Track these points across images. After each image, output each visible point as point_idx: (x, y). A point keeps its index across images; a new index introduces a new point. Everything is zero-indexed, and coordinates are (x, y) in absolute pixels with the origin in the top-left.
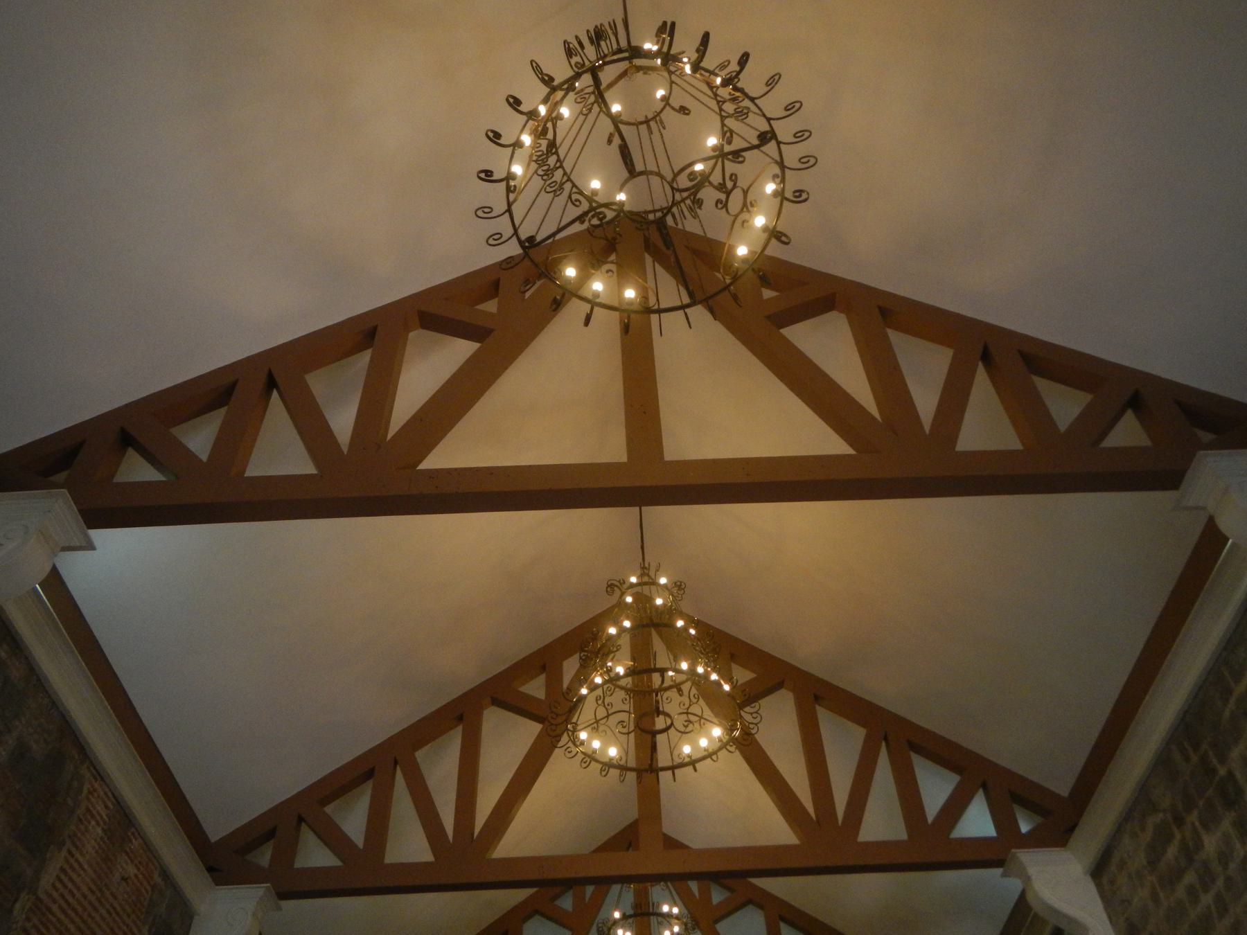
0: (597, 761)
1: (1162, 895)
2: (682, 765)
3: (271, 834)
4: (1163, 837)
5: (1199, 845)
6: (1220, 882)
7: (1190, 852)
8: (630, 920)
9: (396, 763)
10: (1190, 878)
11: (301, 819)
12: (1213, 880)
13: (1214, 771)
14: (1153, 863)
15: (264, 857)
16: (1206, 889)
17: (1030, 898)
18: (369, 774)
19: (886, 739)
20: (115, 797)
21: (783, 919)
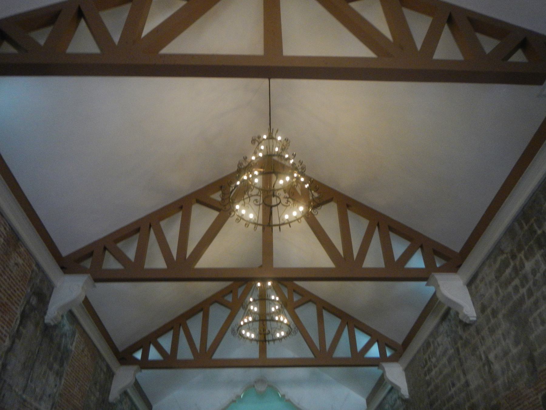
0: (243, 219)
1: (500, 291)
2: (284, 224)
3: (91, 254)
4: (505, 264)
8: (257, 302)
9: (150, 226)
10: (516, 282)
11: (105, 249)
12: (527, 282)
13: (535, 232)
14: (497, 278)
15: (87, 264)
16: (523, 286)
17: (438, 295)
18: (138, 230)
19: (378, 225)
20: (10, 225)
21: (324, 308)
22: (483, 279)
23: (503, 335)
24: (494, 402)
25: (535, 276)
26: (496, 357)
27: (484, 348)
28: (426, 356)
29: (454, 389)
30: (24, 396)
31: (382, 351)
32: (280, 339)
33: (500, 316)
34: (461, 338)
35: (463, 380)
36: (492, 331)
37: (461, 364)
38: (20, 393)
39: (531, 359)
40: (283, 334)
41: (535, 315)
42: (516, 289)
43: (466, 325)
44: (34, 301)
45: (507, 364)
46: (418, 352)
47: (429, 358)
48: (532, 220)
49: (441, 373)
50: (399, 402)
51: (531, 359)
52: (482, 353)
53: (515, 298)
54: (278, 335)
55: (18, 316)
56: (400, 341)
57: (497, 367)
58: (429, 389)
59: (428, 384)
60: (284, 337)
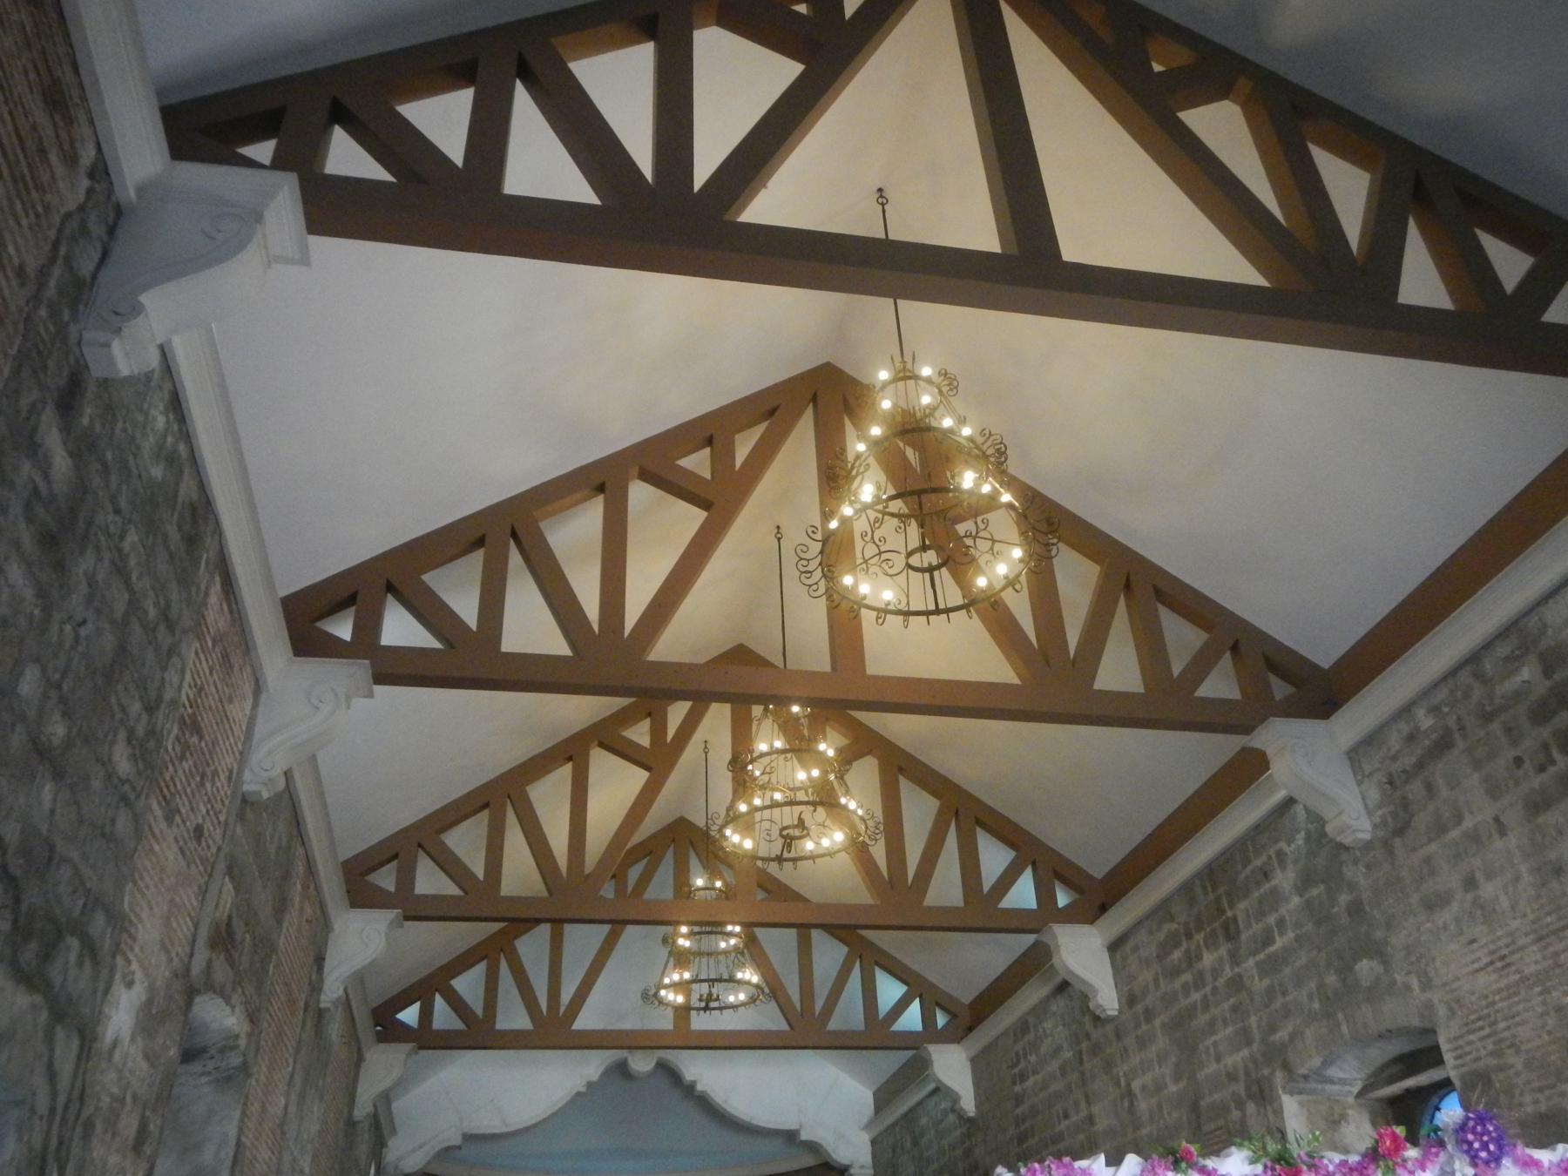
5: (1199, 958)
6: (1208, 989)
7: (1192, 959)
10: (1187, 977)
16: (1197, 988)
18: (486, 805)
22: (1136, 949)
23: (1158, 1056)
25: (1216, 979)
26: (1143, 1088)
27: (1125, 1068)
28: (1019, 1047)
29: (1067, 1122)
31: (928, 1017)
32: (734, 1007)
33: (1157, 1022)
34: (1088, 1036)
35: (1084, 1113)
36: (1142, 1043)
37: (1083, 1082)
39: (1195, 1108)
40: (742, 997)
41: (1209, 1041)
42: (1186, 989)
43: (1097, 1020)
45: (1160, 1107)
46: (1004, 1034)
47: (1025, 1055)
48: (1222, 890)
49: (1044, 1087)
50: (952, 1118)
51: (1195, 1108)
52: (1121, 1074)
53: (1184, 1002)
54: (732, 999)
56: (966, 997)
57: (1143, 1106)
58: (1019, 1111)
59: (1019, 1101)
60: (743, 1004)
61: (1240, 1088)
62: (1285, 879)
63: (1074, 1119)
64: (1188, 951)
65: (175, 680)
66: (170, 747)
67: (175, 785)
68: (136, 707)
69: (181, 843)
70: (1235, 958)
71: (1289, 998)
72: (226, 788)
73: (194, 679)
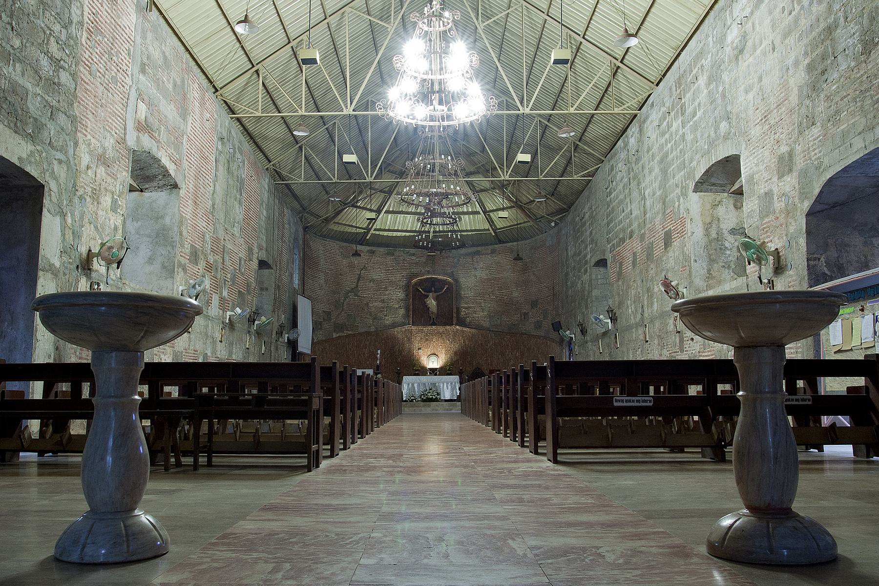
5: (672, 126)
7: (669, 126)
10: (667, 136)
24: (643, 231)
30: (226, 226)
33: (656, 161)
35: (629, 209)
38: (223, 224)
44: (220, 147)
51: (664, 203)
55: (214, 163)
57: (648, 203)
61: (678, 191)
62: (702, 81)
63: (625, 212)
64: (668, 122)
65: (79, 12)
66: (84, 43)
67: (93, 60)
68: (57, 28)
69: (105, 85)
70: (683, 125)
71: (698, 144)
72: (127, 59)
73: (90, 10)
